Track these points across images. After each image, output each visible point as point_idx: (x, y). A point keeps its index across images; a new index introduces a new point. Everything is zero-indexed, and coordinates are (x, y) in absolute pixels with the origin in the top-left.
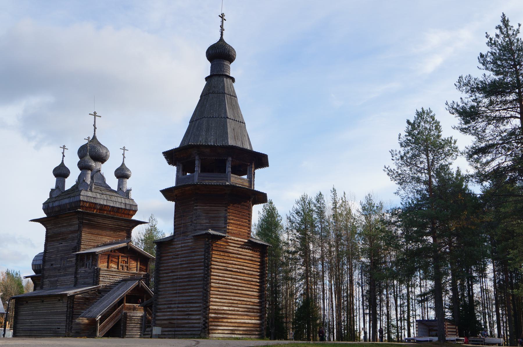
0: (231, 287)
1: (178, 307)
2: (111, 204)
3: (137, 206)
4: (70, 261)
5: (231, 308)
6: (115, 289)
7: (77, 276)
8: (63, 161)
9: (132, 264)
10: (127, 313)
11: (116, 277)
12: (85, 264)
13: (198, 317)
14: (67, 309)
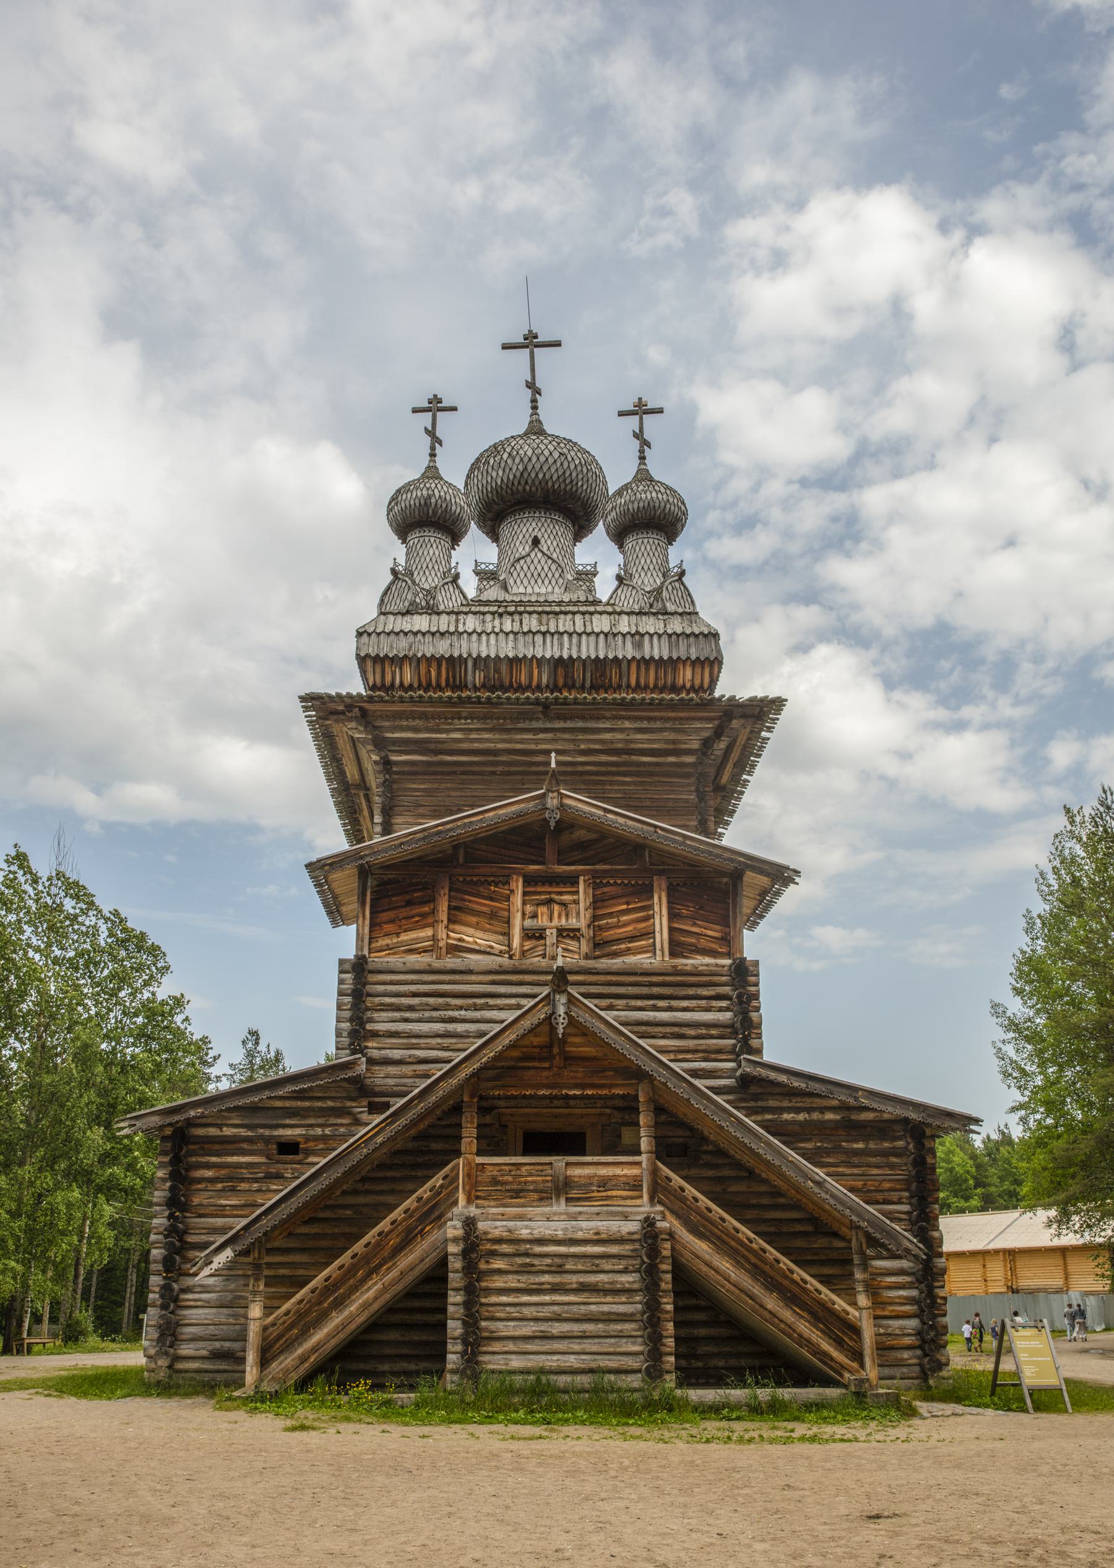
2: (550, 650)
3: (715, 636)
9: (611, 915)
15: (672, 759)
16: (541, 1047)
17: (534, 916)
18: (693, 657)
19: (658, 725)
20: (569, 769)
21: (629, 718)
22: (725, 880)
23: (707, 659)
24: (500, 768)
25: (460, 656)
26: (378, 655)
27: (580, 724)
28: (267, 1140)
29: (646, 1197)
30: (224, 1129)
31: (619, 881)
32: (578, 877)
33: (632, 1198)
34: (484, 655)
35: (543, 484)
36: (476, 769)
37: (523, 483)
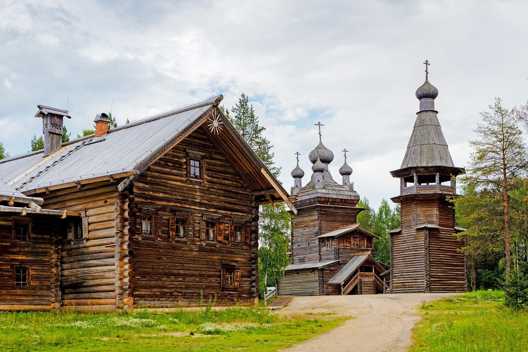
0: (443, 260)
1: (408, 275)
2: (340, 197)
4: (313, 242)
5: (444, 274)
6: (350, 262)
7: (321, 254)
8: (298, 164)
12: (326, 245)
13: (422, 280)
14: (319, 278)
28: (330, 269)
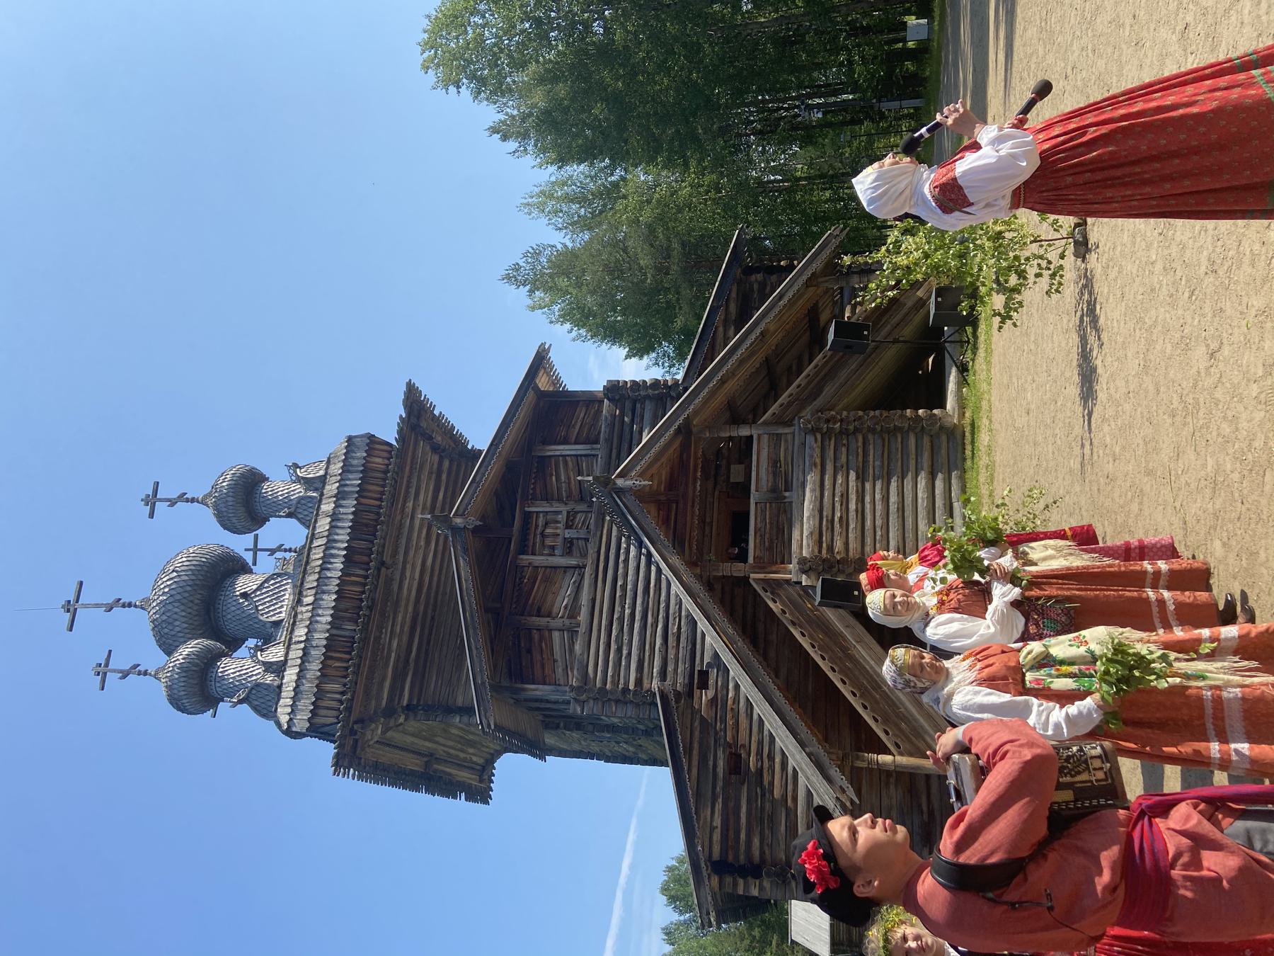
3: (350, 439)
9: (559, 489)
10: (802, 561)
11: (620, 583)
15: (444, 477)
16: (659, 510)
17: (553, 548)
18: (365, 455)
19: (414, 481)
20: (439, 556)
21: (405, 502)
22: (541, 405)
23: (367, 445)
24: (430, 612)
25: (326, 638)
26: (311, 711)
27: (404, 541)
28: (727, 783)
29: (787, 430)
30: (715, 824)
31: (533, 481)
32: (526, 512)
33: (786, 441)
34: (329, 619)
35: (196, 588)
36: (427, 631)
37: (191, 605)
